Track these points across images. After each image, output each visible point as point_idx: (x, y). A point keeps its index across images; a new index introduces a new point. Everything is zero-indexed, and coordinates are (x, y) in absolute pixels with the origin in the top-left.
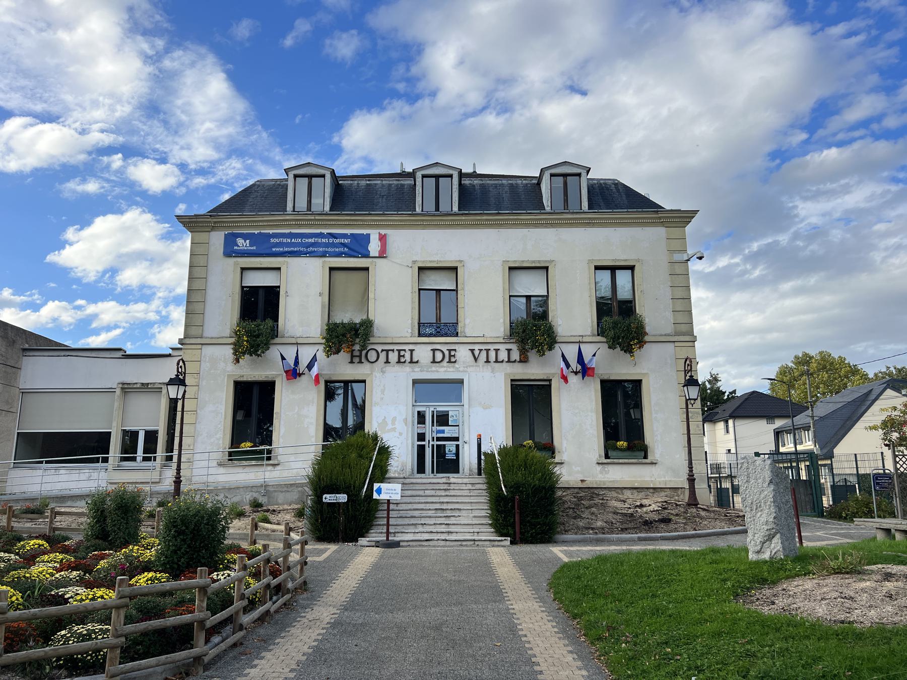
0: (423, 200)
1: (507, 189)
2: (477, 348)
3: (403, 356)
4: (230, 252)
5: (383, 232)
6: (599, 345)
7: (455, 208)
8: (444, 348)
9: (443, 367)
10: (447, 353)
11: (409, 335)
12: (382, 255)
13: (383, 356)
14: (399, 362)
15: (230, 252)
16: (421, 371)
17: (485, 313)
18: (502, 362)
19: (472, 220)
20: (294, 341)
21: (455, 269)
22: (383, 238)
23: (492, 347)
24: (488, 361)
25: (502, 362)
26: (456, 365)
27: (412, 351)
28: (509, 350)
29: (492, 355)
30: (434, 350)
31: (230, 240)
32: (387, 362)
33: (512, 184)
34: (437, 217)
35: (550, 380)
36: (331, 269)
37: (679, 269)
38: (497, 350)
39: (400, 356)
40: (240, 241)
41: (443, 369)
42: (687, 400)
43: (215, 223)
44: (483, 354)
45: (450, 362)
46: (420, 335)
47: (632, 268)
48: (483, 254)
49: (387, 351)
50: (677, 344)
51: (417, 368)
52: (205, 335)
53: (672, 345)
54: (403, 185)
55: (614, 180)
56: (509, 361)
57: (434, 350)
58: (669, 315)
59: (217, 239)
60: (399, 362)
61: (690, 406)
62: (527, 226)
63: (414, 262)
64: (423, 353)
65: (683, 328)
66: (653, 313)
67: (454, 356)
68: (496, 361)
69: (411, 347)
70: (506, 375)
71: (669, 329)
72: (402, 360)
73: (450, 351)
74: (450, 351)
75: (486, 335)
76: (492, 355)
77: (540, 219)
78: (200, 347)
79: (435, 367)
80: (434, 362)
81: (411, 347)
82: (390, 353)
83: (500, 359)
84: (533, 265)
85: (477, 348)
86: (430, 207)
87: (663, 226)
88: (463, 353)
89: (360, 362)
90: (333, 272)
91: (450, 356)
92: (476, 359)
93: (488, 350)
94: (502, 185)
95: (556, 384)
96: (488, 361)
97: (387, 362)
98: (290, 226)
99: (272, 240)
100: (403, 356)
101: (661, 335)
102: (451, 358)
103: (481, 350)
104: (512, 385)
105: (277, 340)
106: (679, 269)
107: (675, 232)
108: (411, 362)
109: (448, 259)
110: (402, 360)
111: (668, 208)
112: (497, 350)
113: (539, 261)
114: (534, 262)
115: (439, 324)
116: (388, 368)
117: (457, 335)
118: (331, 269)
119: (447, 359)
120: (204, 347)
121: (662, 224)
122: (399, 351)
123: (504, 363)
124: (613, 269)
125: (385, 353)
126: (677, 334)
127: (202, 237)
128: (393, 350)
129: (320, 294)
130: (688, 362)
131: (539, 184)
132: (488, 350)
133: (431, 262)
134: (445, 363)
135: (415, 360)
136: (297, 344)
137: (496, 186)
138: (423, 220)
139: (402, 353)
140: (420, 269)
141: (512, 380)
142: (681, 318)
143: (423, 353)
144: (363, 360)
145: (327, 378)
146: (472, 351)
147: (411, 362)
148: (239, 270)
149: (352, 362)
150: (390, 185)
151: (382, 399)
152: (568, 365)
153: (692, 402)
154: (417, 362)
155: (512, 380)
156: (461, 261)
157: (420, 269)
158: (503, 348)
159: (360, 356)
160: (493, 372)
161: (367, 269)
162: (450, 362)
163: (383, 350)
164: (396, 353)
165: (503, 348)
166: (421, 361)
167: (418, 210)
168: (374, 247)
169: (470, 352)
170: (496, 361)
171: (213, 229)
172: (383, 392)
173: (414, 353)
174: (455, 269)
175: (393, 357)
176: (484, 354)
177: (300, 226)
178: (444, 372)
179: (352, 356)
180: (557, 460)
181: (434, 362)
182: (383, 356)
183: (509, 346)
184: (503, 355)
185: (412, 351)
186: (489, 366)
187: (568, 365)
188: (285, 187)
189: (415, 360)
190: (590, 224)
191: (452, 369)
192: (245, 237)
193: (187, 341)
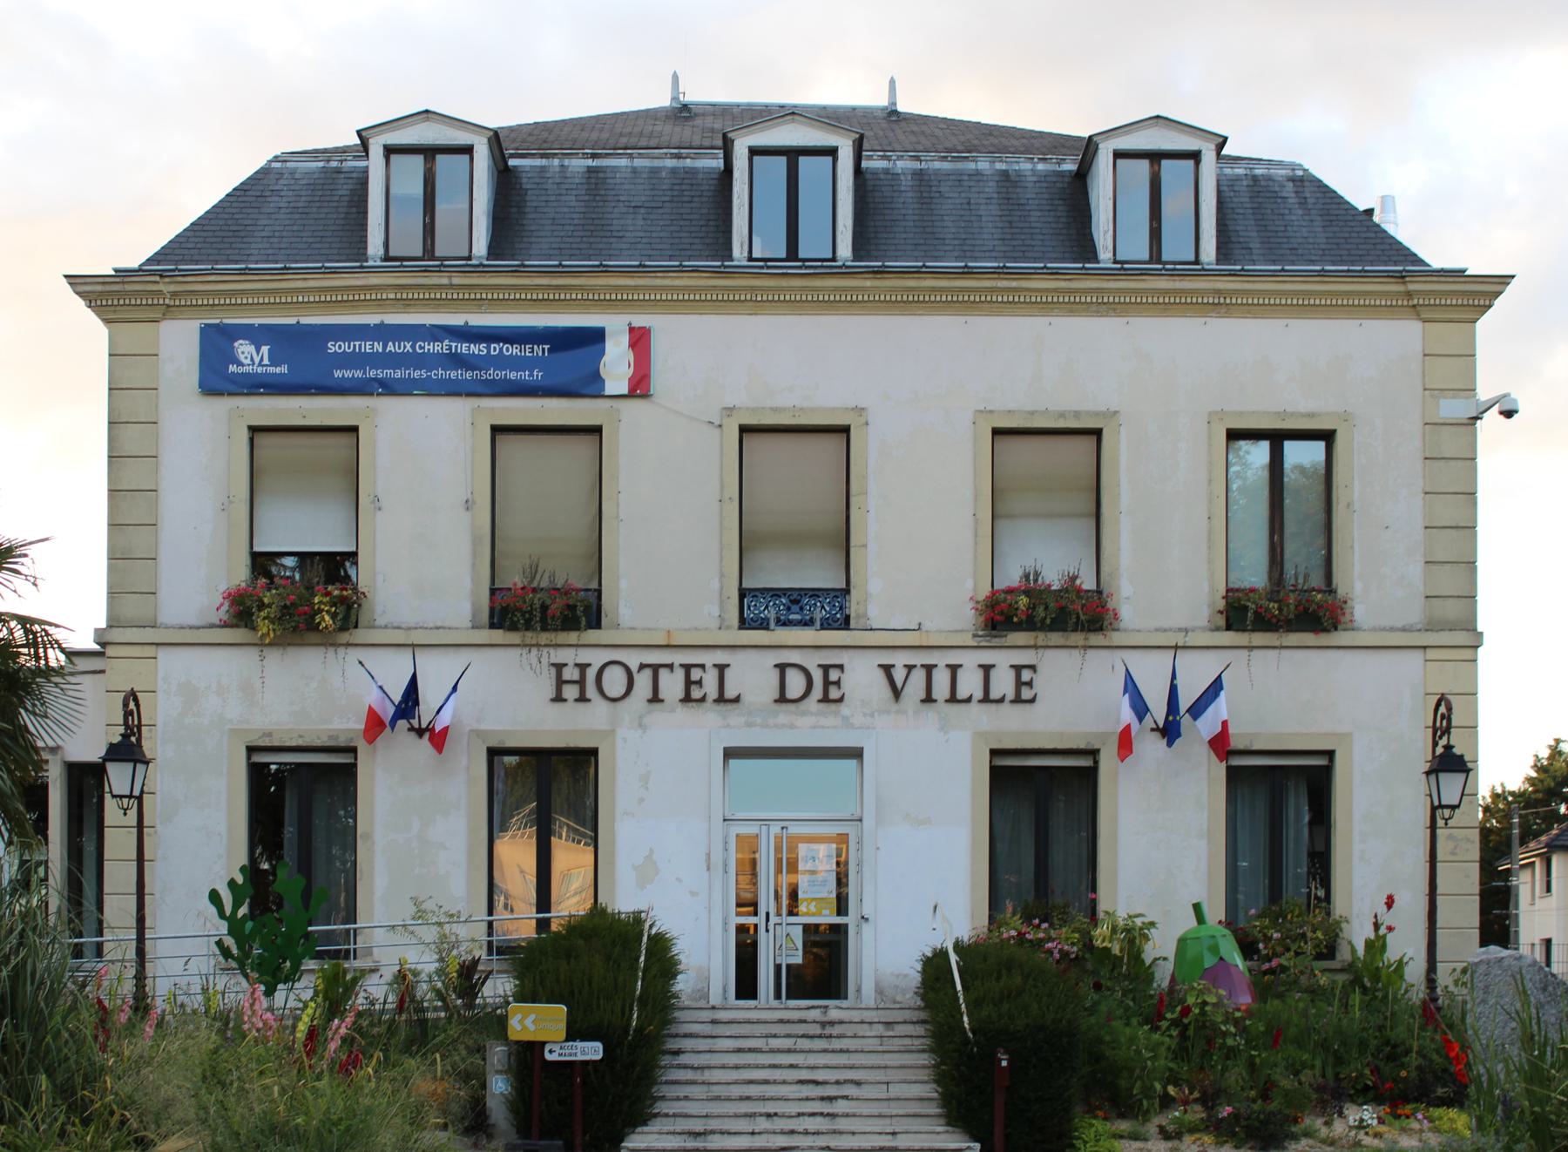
0: (754, 229)
1: (991, 188)
2: (899, 660)
3: (699, 683)
4: (218, 378)
5: (640, 321)
6: (1229, 655)
7: (845, 250)
8: (812, 662)
9: (804, 713)
10: (817, 676)
11: (715, 624)
12: (640, 387)
13: (643, 681)
14: (687, 699)
15: (218, 378)
16: (749, 725)
17: (922, 556)
18: (969, 700)
19: (893, 290)
20: (400, 637)
21: (845, 430)
22: (640, 340)
23: (941, 660)
24: (929, 699)
25: (969, 700)
26: (844, 709)
27: (721, 668)
28: (987, 669)
29: (941, 680)
30: (782, 668)
31: (216, 344)
32: (655, 699)
33: (1005, 173)
34: (794, 274)
35: (1094, 753)
36: (496, 430)
37: (1449, 443)
38: (954, 669)
39: (689, 683)
40: (244, 349)
41: (807, 721)
42: (1434, 809)
43: (174, 294)
44: (918, 681)
45: (825, 699)
46: (744, 624)
47: (1327, 437)
48: (922, 384)
49: (655, 668)
50: (1431, 654)
51: (735, 716)
52: (160, 620)
53: (1419, 654)
54: (693, 172)
55: (1293, 166)
56: (986, 699)
57: (782, 668)
58: (1415, 570)
59: (179, 341)
60: (687, 699)
61: (1440, 823)
62: (1045, 306)
63: (729, 411)
64: (752, 675)
65: (1451, 610)
66: (1377, 571)
67: (838, 683)
68: (953, 699)
69: (721, 657)
70: (978, 735)
71: (1414, 613)
72: (696, 693)
73: (826, 669)
74: (826, 669)
75: (927, 625)
76: (941, 680)
77: (1085, 291)
78: (149, 651)
79: (785, 714)
80: (782, 699)
81: (721, 657)
82: (663, 673)
83: (961, 694)
84: (1061, 424)
85: (899, 660)
86: (771, 244)
87: (1418, 317)
88: (861, 676)
89: (582, 699)
90: (507, 443)
91: (827, 683)
92: (897, 693)
93: (929, 669)
94: (978, 173)
95: (1108, 762)
96: (929, 699)
97: (655, 699)
98: (380, 305)
99: (333, 347)
100: (699, 683)
101: (1392, 629)
102: (829, 690)
103: (910, 668)
104: (993, 769)
105: (360, 635)
106: (1449, 443)
107: (1446, 333)
108: (721, 699)
109: (820, 399)
110: (696, 693)
111: (1436, 263)
112: (954, 669)
113: (1077, 414)
114: (1062, 415)
115: (797, 597)
116: (658, 715)
117: (845, 624)
118: (496, 430)
119: (817, 691)
120: (162, 653)
121: (1415, 311)
122: (687, 668)
123: (974, 706)
124: (1277, 438)
125: (648, 673)
126: (1431, 626)
127: (136, 335)
128: (670, 667)
129: (468, 505)
130: (1442, 709)
131: (1081, 177)
132: (929, 669)
133: (775, 410)
134: (812, 702)
135: (730, 693)
136: (413, 646)
137: (958, 178)
138: (753, 289)
139: (696, 674)
140: (744, 430)
141: (994, 753)
142: (1447, 582)
143: (752, 675)
144: (591, 691)
145: (494, 743)
146: (887, 669)
147: (721, 699)
148: (244, 435)
149: (559, 698)
150: (654, 171)
151: (642, 800)
152: (1140, 709)
153: (1447, 812)
154: (737, 700)
155: (994, 753)
156: (860, 410)
157: (744, 430)
158: (970, 662)
159: (581, 683)
160: (943, 729)
161: (596, 430)
162: (825, 699)
163: (642, 667)
164: (680, 674)
165: (970, 662)
166: (745, 699)
167: (739, 252)
168: (616, 364)
169: (880, 674)
170: (953, 699)
171: (169, 311)
172: (645, 779)
173: (727, 672)
174: (845, 430)
175: (672, 685)
176: (919, 677)
177: (407, 305)
178: (810, 726)
179: (560, 683)
180: (1148, 962)
181: (782, 699)
182: (643, 681)
183: (987, 657)
184: (970, 683)
185: (721, 668)
186: (930, 712)
187: (1140, 709)
188: (364, 183)
189: (730, 693)
190: (1220, 306)
191: (831, 721)
192: (257, 335)
193: (117, 635)
